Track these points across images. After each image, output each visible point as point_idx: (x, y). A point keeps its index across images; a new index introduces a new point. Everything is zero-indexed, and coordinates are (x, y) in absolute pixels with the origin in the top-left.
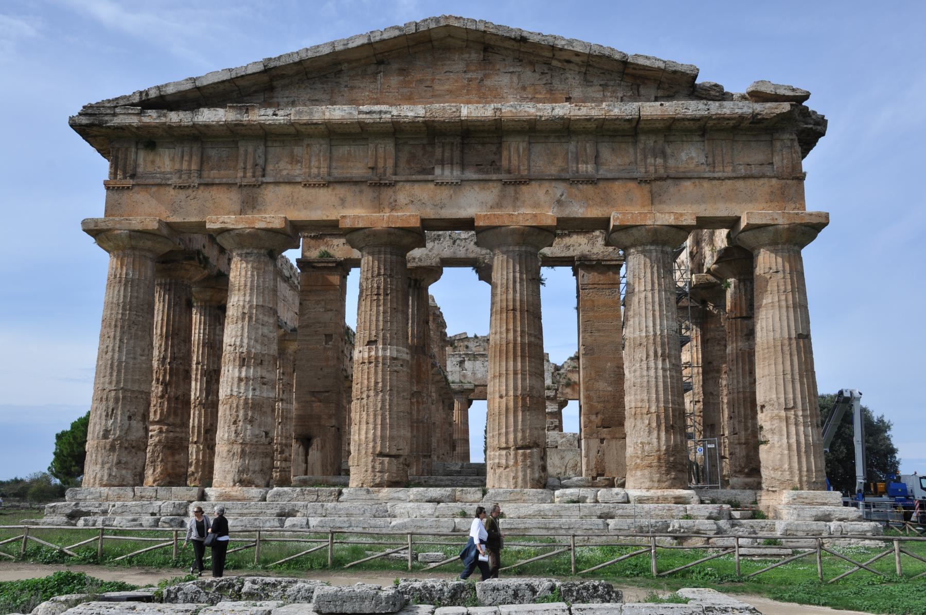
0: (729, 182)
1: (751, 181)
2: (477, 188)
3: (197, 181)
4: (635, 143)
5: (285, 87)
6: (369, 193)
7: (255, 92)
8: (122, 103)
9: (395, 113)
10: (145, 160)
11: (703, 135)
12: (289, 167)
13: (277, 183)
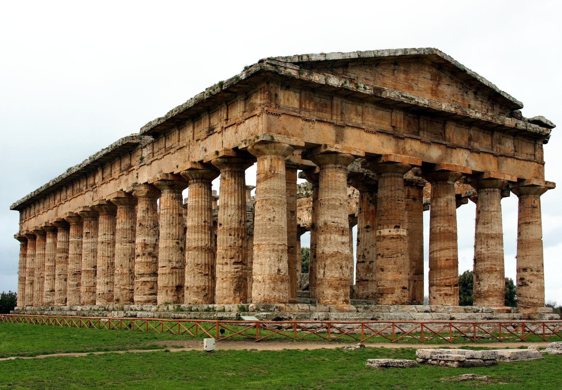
0: (522, 161)
1: (529, 163)
2: (436, 146)
3: (314, 118)
4: (492, 135)
5: (353, 67)
6: (393, 142)
7: (340, 66)
8: (289, 61)
9: (416, 100)
10: (284, 97)
11: (514, 136)
12: (355, 117)
13: (353, 127)
